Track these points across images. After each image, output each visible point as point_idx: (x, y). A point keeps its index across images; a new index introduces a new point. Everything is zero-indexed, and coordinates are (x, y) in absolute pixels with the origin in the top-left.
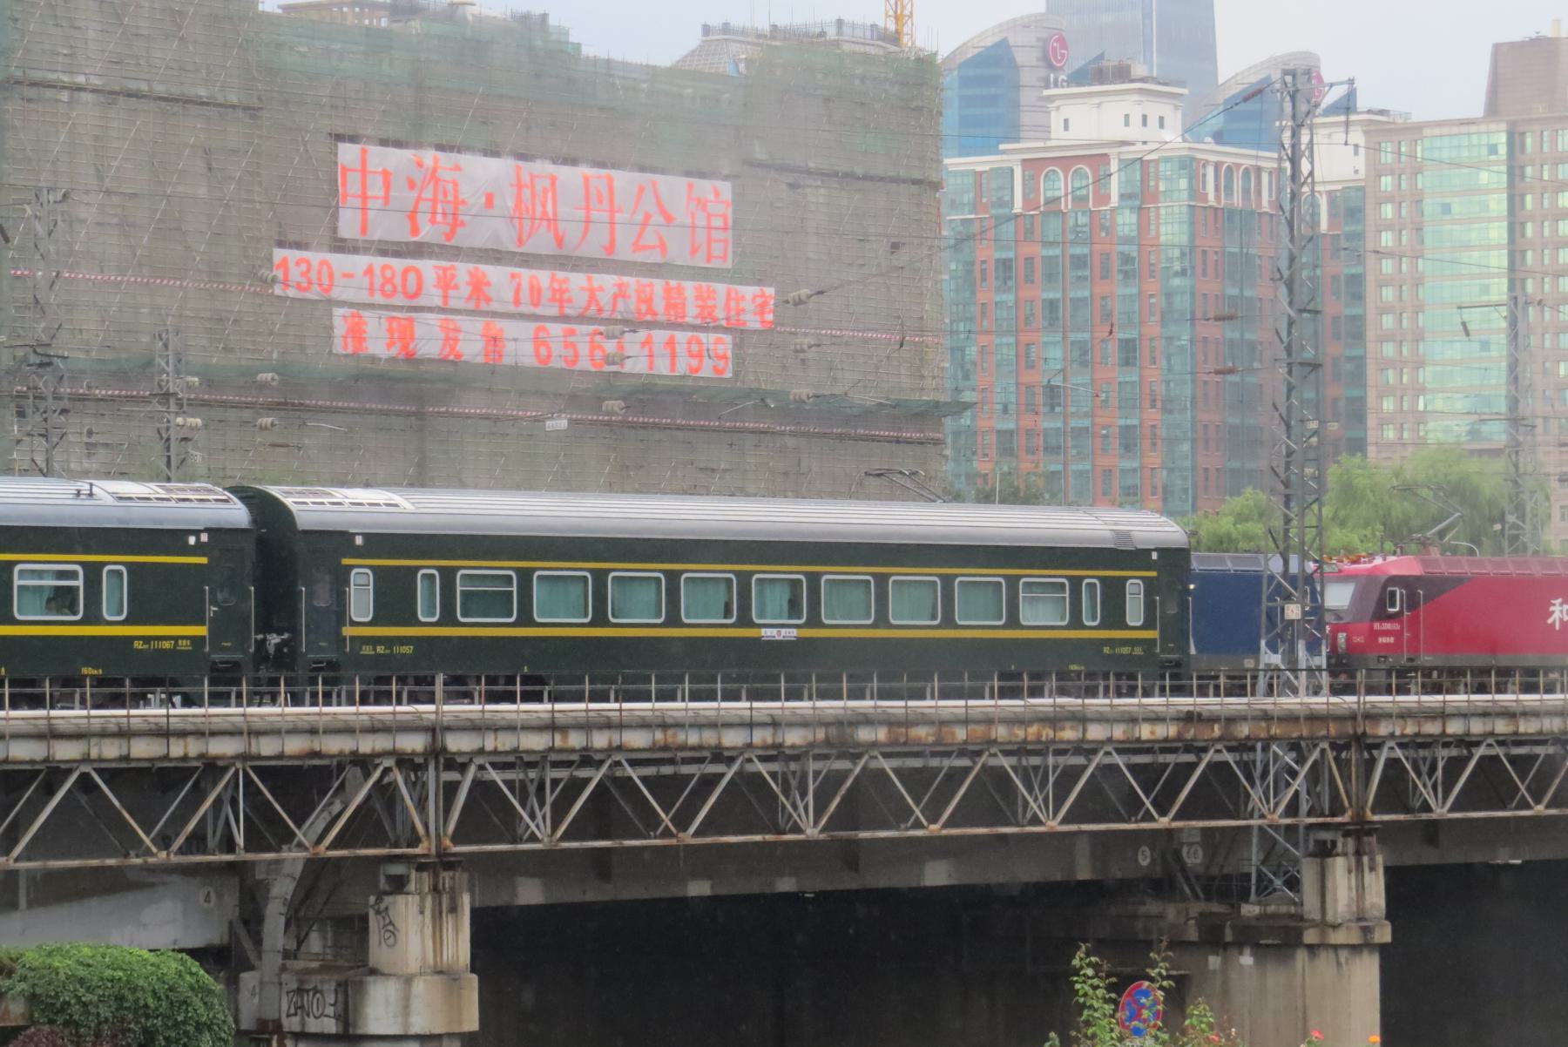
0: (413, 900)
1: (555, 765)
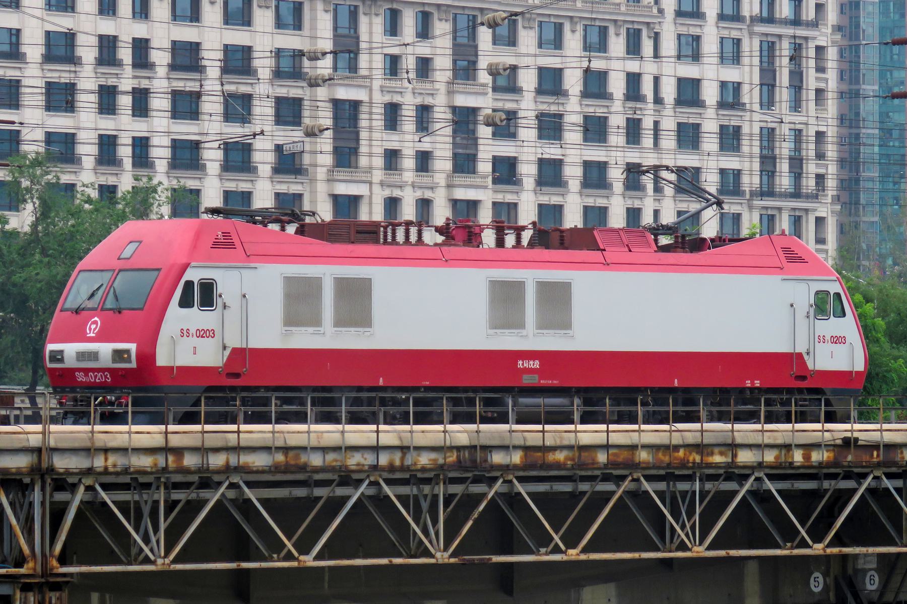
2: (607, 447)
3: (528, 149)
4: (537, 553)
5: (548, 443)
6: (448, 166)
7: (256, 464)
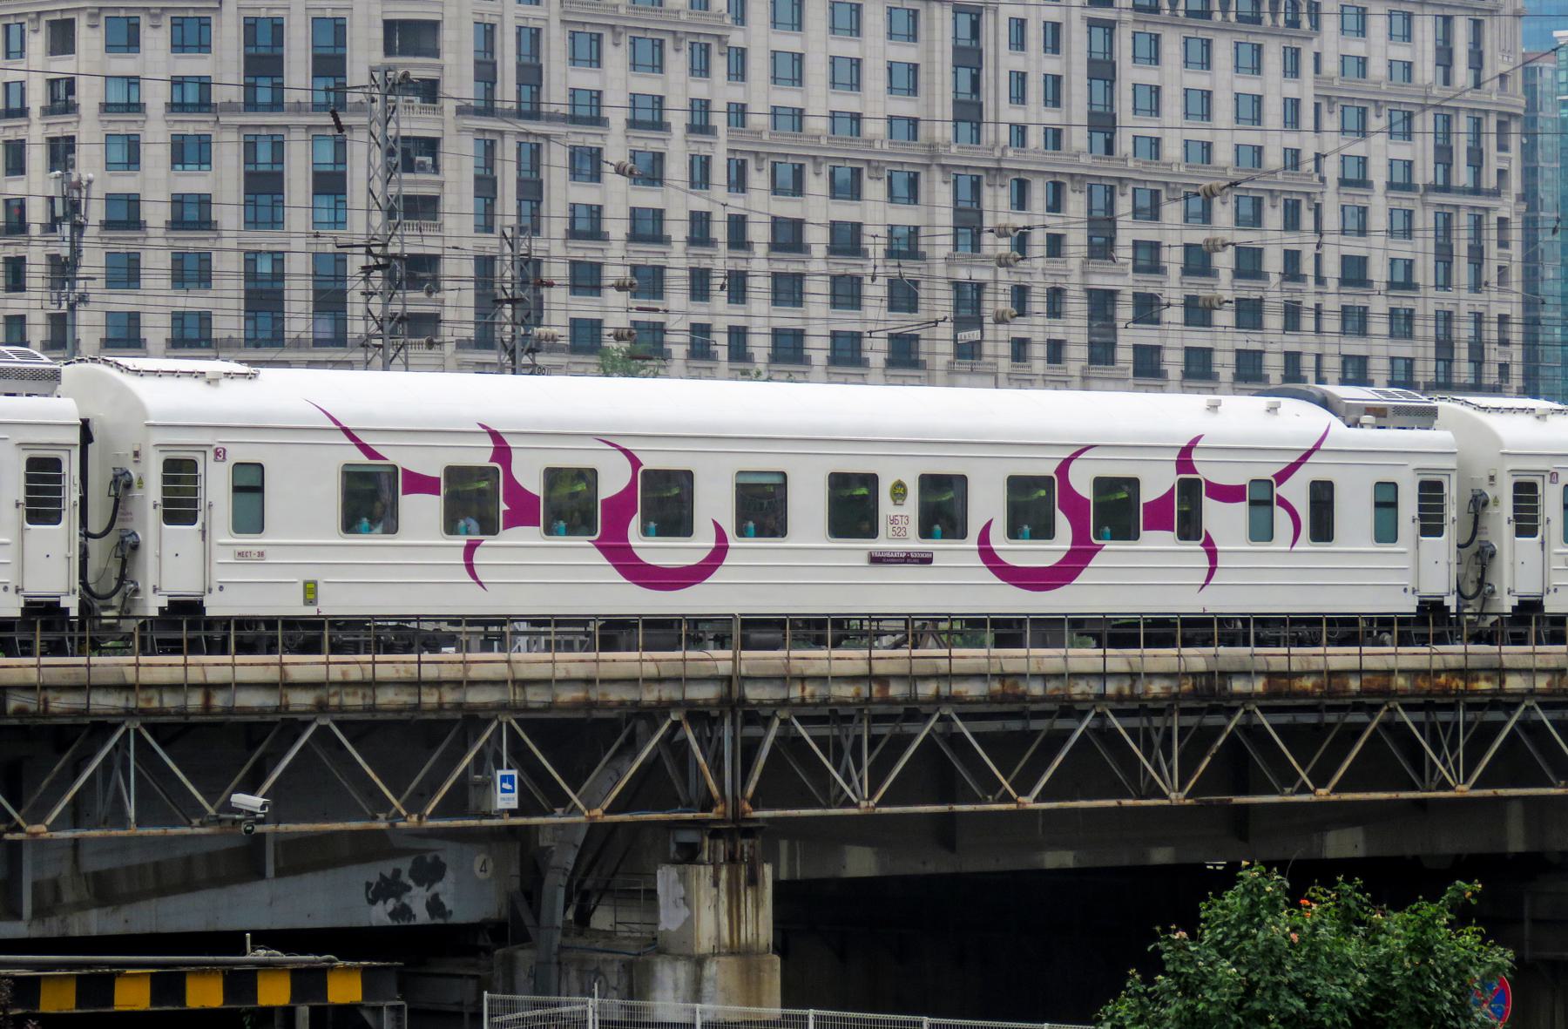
0: (706, 872)
1: (876, 719)
2: (1360, 672)
3: (1174, 336)
4: (1282, 793)
5: (1294, 668)
6: (1083, 353)
7: (972, 693)
